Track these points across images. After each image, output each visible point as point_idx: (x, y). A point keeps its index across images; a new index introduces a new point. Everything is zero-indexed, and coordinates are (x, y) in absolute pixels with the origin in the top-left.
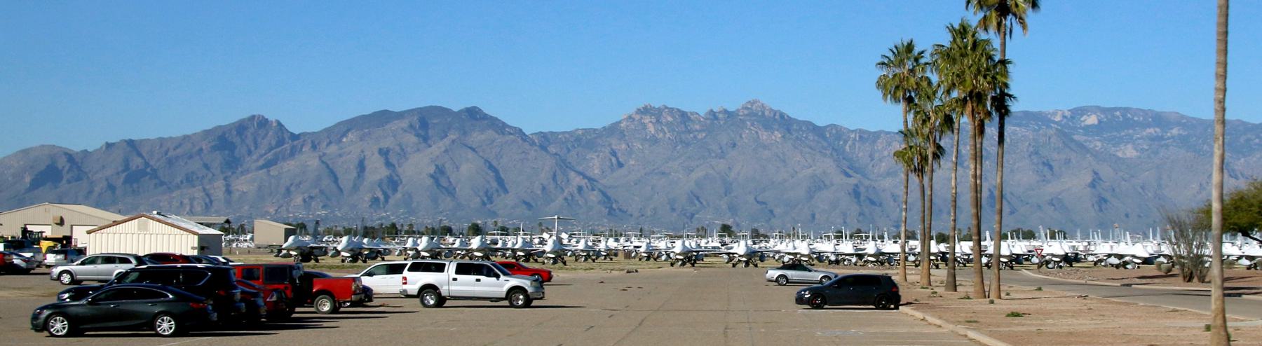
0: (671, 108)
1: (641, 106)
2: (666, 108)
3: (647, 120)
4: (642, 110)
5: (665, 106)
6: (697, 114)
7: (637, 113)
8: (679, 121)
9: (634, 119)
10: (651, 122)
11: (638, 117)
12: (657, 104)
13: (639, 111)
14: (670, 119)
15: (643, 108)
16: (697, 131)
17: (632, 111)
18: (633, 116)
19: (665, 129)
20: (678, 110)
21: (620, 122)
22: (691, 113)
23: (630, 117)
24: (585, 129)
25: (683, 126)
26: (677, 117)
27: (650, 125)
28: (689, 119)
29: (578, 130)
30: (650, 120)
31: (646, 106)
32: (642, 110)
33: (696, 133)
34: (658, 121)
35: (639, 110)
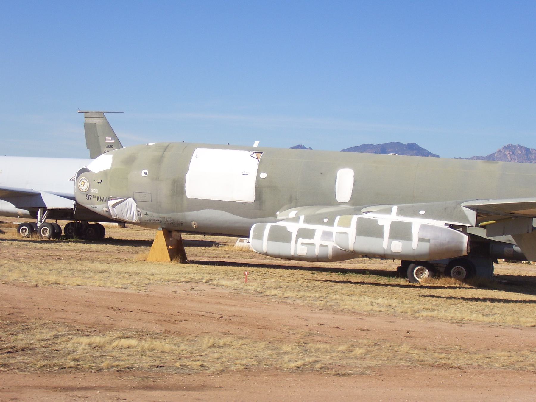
0: (521, 146)
1: (506, 144)
2: (519, 146)
3: (507, 153)
4: (507, 147)
5: (518, 145)
6: (535, 150)
7: (503, 148)
8: (524, 153)
9: (501, 152)
10: (509, 154)
11: (503, 151)
12: (515, 144)
13: (505, 148)
14: (519, 152)
15: (507, 146)
16: (532, 159)
17: (501, 147)
18: (501, 151)
19: (516, 158)
20: (525, 147)
21: (494, 154)
22: (531, 149)
23: (500, 151)
24: (478, 157)
25: (526, 156)
26: (523, 151)
27: (509, 155)
28: (531, 152)
29: (475, 157)
30: (509, 153)
31: (509, 145)
32: (507, 147)
33: (532, 160)
34: (513, 153)
35: (505, 146)
